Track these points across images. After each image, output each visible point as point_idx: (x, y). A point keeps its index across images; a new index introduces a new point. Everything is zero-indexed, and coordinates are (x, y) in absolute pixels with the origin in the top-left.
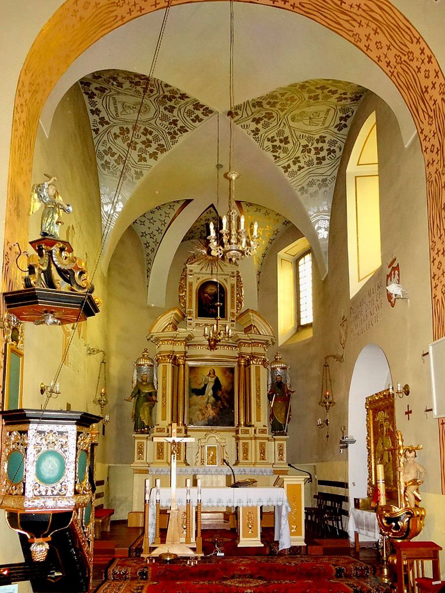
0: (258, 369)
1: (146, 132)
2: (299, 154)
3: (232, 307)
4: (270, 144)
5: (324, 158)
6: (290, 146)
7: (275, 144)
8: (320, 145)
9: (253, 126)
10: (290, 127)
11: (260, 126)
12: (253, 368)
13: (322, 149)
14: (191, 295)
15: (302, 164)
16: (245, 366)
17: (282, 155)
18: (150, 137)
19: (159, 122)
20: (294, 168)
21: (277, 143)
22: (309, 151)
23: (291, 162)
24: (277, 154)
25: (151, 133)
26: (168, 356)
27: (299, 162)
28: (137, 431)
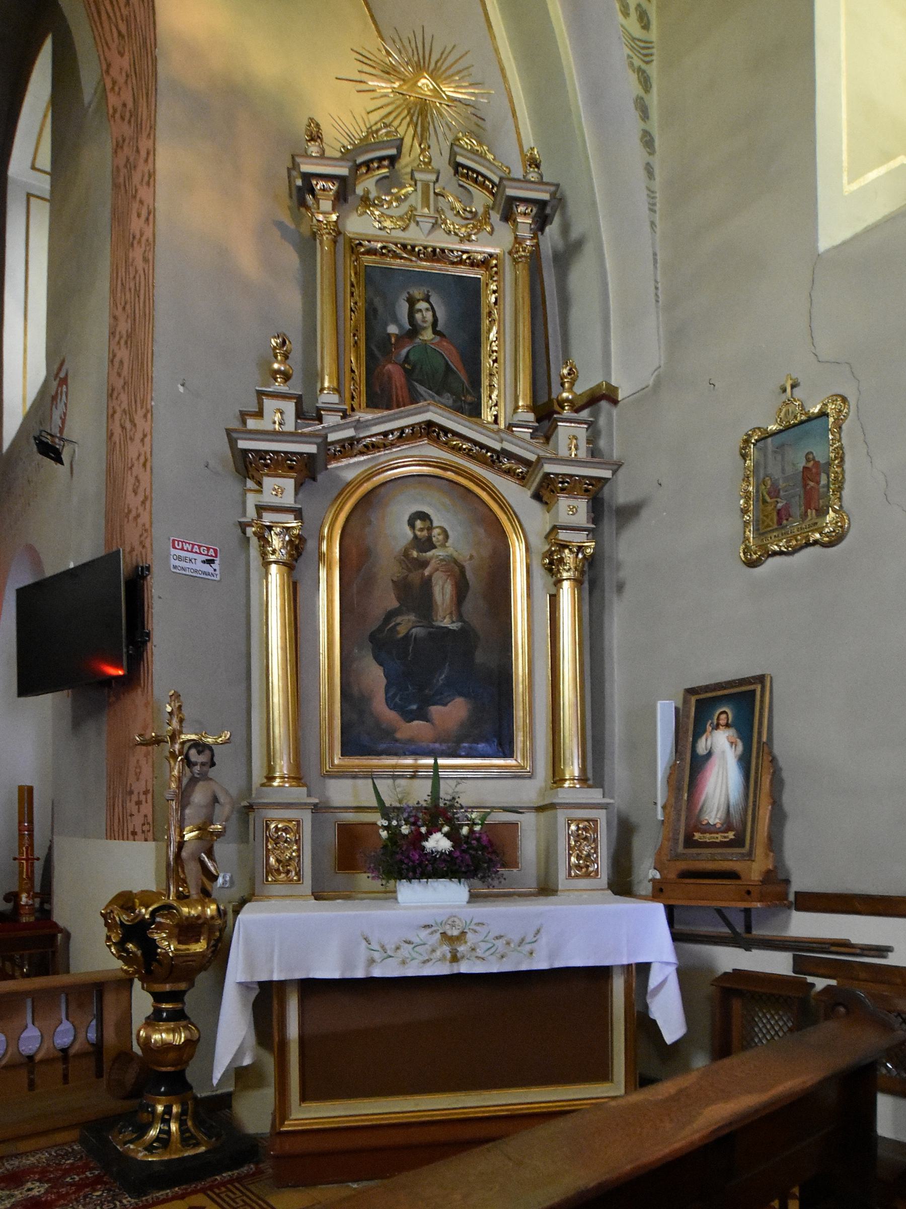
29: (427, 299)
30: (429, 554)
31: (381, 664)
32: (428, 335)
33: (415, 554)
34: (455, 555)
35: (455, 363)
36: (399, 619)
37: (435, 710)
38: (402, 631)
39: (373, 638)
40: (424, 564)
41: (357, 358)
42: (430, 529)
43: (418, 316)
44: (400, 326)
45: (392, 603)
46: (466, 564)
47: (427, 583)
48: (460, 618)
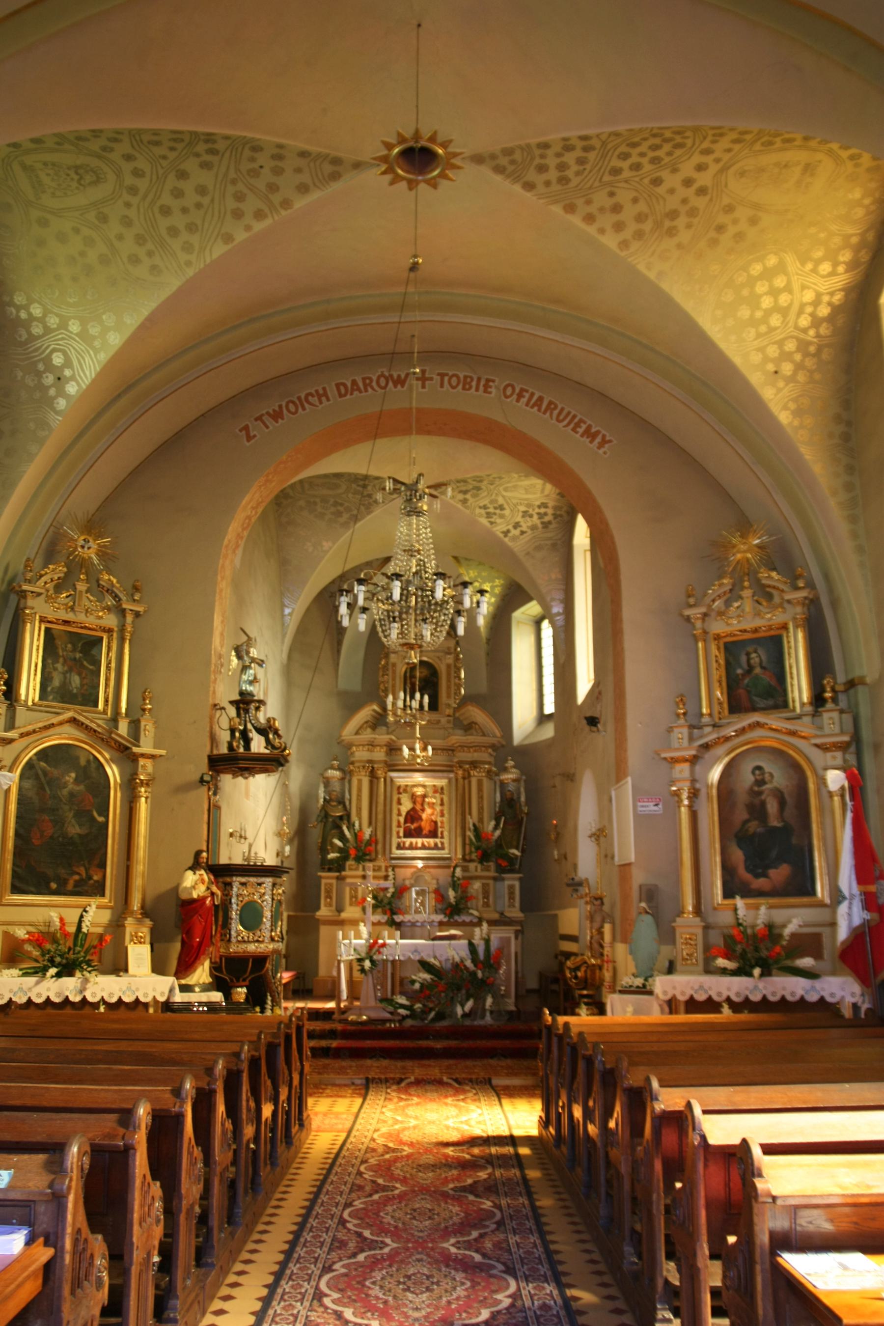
1: (336, 504)
2: (519, 519)
3: (449, 696)
4: (483, 511)
5: (550, 522)
6: (507, 512)
7: (488, 510)
8: (542, 510)
9: (461, 496)
10: (503, 497)
11: (468, 496)
13: (546, 514)
14: (394, 679)
15: (524, 529)
16: (464, 778)
17: (499, 521)
18: (341, 508)
19: (350, 495)
20: (517, 532)
21: (491, 510)
22: (531, 516)
23: (510, 527)
24: (492, 520)
25: (341, 505)
26: (364, 767)
27: (520, 526)
28: (324, 869)
29: (756, 652)
30: (764, 787)
31: (741, 848)
32: (758, 670)
33: (756, 789)
34: (778, 786)
35: (773, 683)
36: (750, 824)
37: (772, 872)
38: (751, 830)
39: (736, 836)
40: (760, 793)
41: (722, 693)
42: (763, 774)
43: (752, 661)
44: (743, 669)
45: (745, 816)
46: (785, 791)
47: (763, 804)
48: (783, 821)
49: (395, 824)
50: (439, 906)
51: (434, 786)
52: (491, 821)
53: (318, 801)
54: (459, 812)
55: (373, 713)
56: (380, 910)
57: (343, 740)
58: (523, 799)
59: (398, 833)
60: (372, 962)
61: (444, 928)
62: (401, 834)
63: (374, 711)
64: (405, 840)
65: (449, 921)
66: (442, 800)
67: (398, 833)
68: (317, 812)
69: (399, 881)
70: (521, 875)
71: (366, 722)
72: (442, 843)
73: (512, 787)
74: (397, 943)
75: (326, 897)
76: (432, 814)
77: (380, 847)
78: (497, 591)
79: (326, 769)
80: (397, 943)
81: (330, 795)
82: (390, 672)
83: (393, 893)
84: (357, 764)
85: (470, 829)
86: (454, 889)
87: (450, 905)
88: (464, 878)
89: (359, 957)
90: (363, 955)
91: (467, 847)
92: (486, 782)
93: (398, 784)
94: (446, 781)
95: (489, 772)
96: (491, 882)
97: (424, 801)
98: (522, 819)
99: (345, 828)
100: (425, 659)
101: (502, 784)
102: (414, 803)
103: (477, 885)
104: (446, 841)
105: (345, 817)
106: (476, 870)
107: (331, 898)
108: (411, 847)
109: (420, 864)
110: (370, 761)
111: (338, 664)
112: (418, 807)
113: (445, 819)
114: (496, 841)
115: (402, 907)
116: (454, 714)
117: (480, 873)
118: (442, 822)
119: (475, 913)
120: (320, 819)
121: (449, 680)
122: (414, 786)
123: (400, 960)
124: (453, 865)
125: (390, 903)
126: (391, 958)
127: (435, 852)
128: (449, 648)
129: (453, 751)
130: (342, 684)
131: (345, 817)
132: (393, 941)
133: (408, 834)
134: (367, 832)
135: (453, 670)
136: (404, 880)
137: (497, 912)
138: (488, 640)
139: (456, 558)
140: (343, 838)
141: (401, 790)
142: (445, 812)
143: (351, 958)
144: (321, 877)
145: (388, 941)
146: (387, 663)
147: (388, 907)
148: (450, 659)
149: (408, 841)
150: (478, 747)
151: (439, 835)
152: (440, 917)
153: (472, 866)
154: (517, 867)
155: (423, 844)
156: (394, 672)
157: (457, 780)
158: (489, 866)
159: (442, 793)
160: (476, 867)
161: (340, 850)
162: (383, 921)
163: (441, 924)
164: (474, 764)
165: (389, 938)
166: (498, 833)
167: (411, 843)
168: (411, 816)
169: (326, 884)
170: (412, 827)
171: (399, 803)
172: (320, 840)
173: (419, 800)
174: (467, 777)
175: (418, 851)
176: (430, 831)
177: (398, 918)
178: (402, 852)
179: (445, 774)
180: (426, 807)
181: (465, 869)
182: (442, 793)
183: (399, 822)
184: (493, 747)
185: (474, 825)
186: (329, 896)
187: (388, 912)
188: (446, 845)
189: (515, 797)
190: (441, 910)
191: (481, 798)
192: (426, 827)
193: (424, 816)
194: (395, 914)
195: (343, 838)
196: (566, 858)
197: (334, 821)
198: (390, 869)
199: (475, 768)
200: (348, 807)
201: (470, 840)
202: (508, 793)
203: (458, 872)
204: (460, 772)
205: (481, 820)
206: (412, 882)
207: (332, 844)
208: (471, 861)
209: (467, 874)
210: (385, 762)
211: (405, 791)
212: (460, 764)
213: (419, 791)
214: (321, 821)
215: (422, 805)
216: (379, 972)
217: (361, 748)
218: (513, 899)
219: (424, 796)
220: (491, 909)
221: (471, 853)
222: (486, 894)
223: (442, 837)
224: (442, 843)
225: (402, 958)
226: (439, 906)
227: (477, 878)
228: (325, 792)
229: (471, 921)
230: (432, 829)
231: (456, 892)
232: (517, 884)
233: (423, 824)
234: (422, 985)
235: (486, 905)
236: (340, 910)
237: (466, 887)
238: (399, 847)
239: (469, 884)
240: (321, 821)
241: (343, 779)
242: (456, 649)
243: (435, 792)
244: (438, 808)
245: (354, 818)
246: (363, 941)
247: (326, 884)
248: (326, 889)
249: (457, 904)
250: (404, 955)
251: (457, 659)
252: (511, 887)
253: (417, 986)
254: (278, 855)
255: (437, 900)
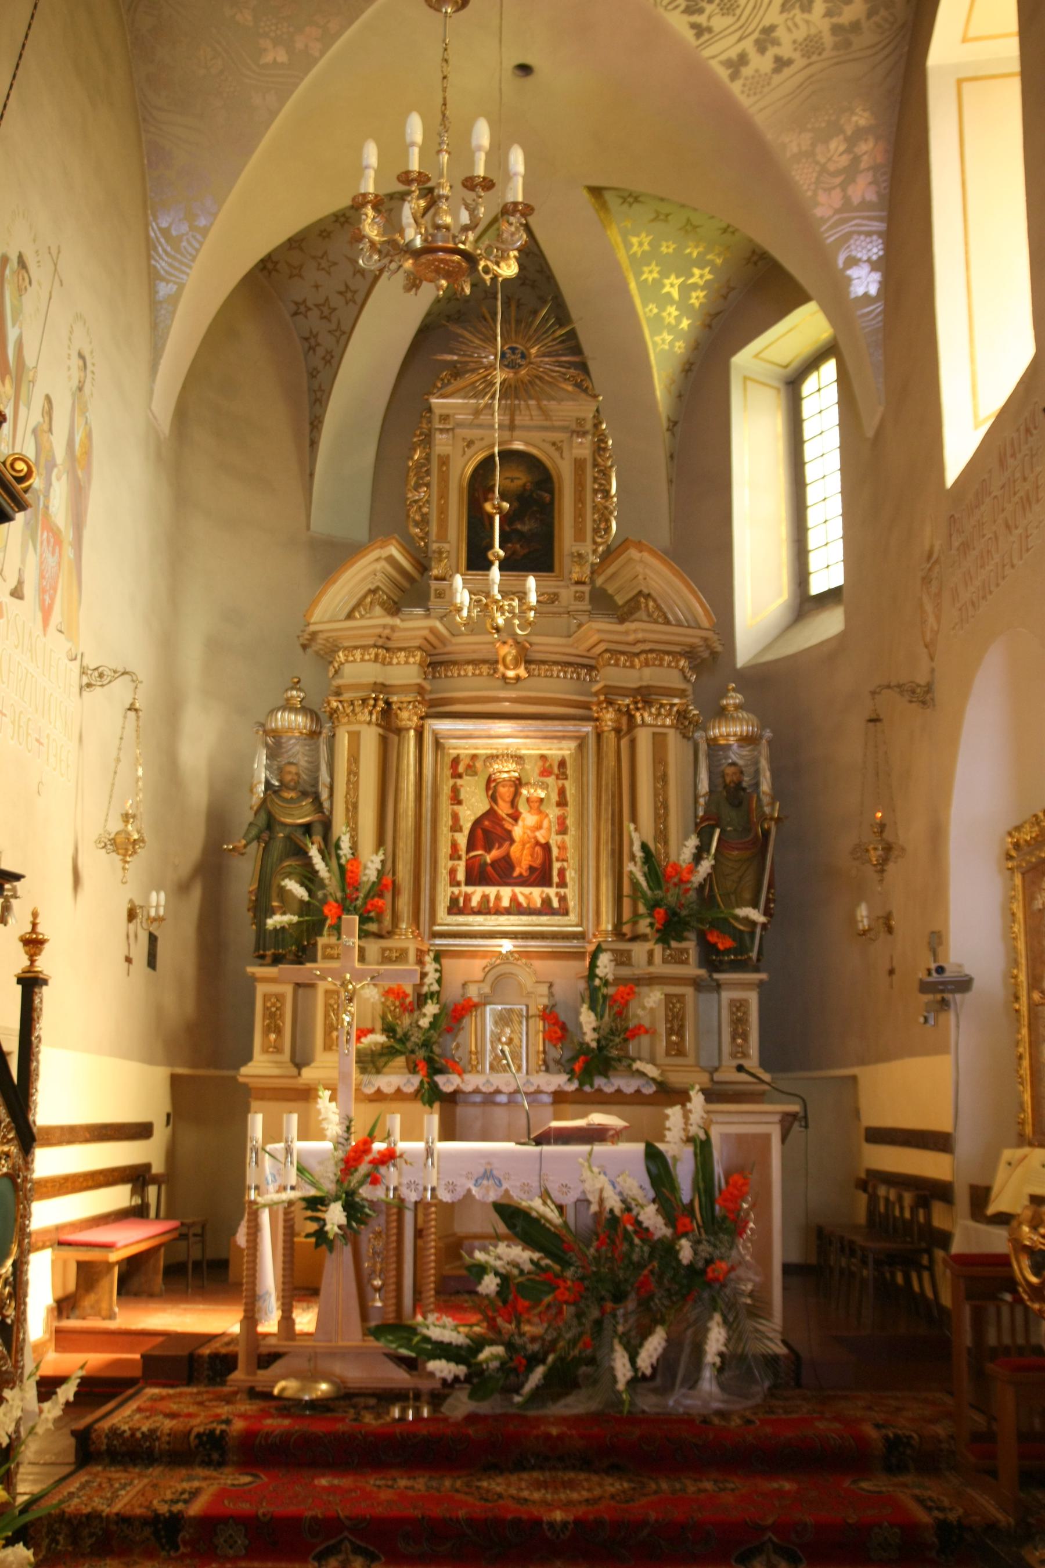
0: (659, 741)
3: (579, 536)
12: (644, 739)
14: (443, 495)
28: (262, 957)
49: (444, 850)
50: (555, 1053)
51: (543, 757)
52: (686, 837)
53: (252, 790)
54: (606, 815)
55: (390, 569)
56: (400, 1061)
57: (314, 635)
58: (765, 787)
59: (452, 872)
60: (352, 1208)
61: (569, 1108)
62: (461, 876)
63: (391, 560)
64: (470, 889)
65: (579, 1090)
66: (562, 792)
67: (452, 872)
68: (249, 816)
69: (452, 994)
70: (763, 976)
71: (373, 591)
72: (563, 899)
73: (737, 755)
74: (429, 1152)
75: (267, 1030)
76: (539, 827)
77: (404, 903)
78: (697, 298)
79: (272, 712)
80: (429, 1152)
81: (280, 772)
82: (434, 479)
83: (436, 1017)
84: (347, 696)
85: (633, 857)
86: (592, 1008)
87: (583, 1049)
88: (618, 980)
89: (312, 1192)
90: (329, 1186)
91: (626, 903)
92: (673, 738)
93: (454, 752)
94: (573, 745)
95: (682, 715)
96: (689, 991)
97: (517, 794)
98: (766, 834)
99: (314, 852)
100: (518, 446)
101: (713, 744)
102: (493, 798)
103: (653, 998)
104: (571, 892)
105: (318, 829)
106: (650, 961)
107: (279, 1031)
108: (485, 909)
109: (507, 946)
110: (382, 687)
111: (312, 475)
112: (503, 809)
113: (569, 839)
114: (701, 887)
115: (458, 1055)
116: (592, 581)
117: (659, 968)
118: (562, 847)
119: (652, 1071)
120: (254, 832)
121: (579, 498)
122: (493, 757)
123: (440, 1205)
124: (591, 948)
125: (426, 1044)
126: (412, 1197)
127: (544, 919)
128: (580, 421)
129: (591, 668)
130: (322, 523)
131: (318, 829)
132: (420, 1146)
133: (477, 875)
134: (371, 865)
135: (590, 472)
136: (464, 985)
137: (703, 1069)
138: (673, 424)
139: (596, 192)
140: (309, 878)
141: (461, 769)
142: (569, 822)
143: (290, 1195)
144: (254, 979)
145: (402, 1146)
146: (428, 458)
147: (421, 1054)
148: (583, 448)
149: (477, 893)
150: (656, 654)
151: (556, 879)
152: (558, 1081)
153: (639, 951)
154: (754, 955)
155: (514, 899)
156: (444, 479)
157: (599, 736)
158: (686, 951)
159: (562, 775)
160: (651, 954)
161: (304, 908)
162: (409, 1089)
163: (559, 1097)
164: (645, 696)
165: (403, 1138)
166: (706, 866)
167: (485, 898)
168: (486, 832)
169: (266, 997)
170: (489, 859)
171: (456, 799)
172: (255, 886)
173: (505, 791)
174: (627, 727)
175: (503, 919)
176: (531, 869)
177: (447, 1083)
178: (461, 919)
179: (570, 727)
180: (522, 807)
181: (622, 959)
182: (562, 775)
183: (454, 846)
184: (690, 654)
185: (644, 847)
186: (274, 1026)
187: (423, 1068)
188: (572, 903)
189: (746, 781)
190: (558, 1062)
191: (661, 778)
192: (523, 858)
193: (517, 832)
194: (441, 1071)
195: (309, 878)
196: (890, 930)
197: (288, 838)
198: (428, 959)
199: (648, 703)
200: (326, 805)
201: (635, 885)
202: (730, 770)
203: (605, 965)
204: (609, 716)
205: (662, 835)
206: (486, 989)
207: (284, 894)
208: (635, 938)
209: (625, 972)
210: (421, 690)
211: (471, 770)
212: (610, 696)
213: (506, 770)
214: (258, 838)
215: (513, 803)
216: (378, 1234)
217: (358, 654)
218: (745, 1036)
219: (518, 784)
220: (690, 1060)
221: (636, 916)
222: (676, 1023)
223: (563, 884)
224: (563, 899)
225: (445, 1196)
226: (555, 1053)
227: (652, 980)
228: (268, 767)
229: (638, 1091)
230: (537, 863)
231: (600, 1016)
232: (753, 998)
233: (515, 850)
234: (505, 1279)
235: (677, 1050)
236: (300, 1060)
237: (626, 1004)
238: (455, 908)
239: (631, 993)
240: (258, 838)
241: (314, 735)
242: (597, 425)
243: (546, 772)
244: (553, 812)
245: (340, 830)
246: (327, 1145)
247: (266, 997)
248: (266, 1008)
249: (600, 1048)
250: (452, 1188)
251: (599, 448)
252: (739, 1007)
253: (489, 1284)
254: (132, 915)
255: (548, 1037)
